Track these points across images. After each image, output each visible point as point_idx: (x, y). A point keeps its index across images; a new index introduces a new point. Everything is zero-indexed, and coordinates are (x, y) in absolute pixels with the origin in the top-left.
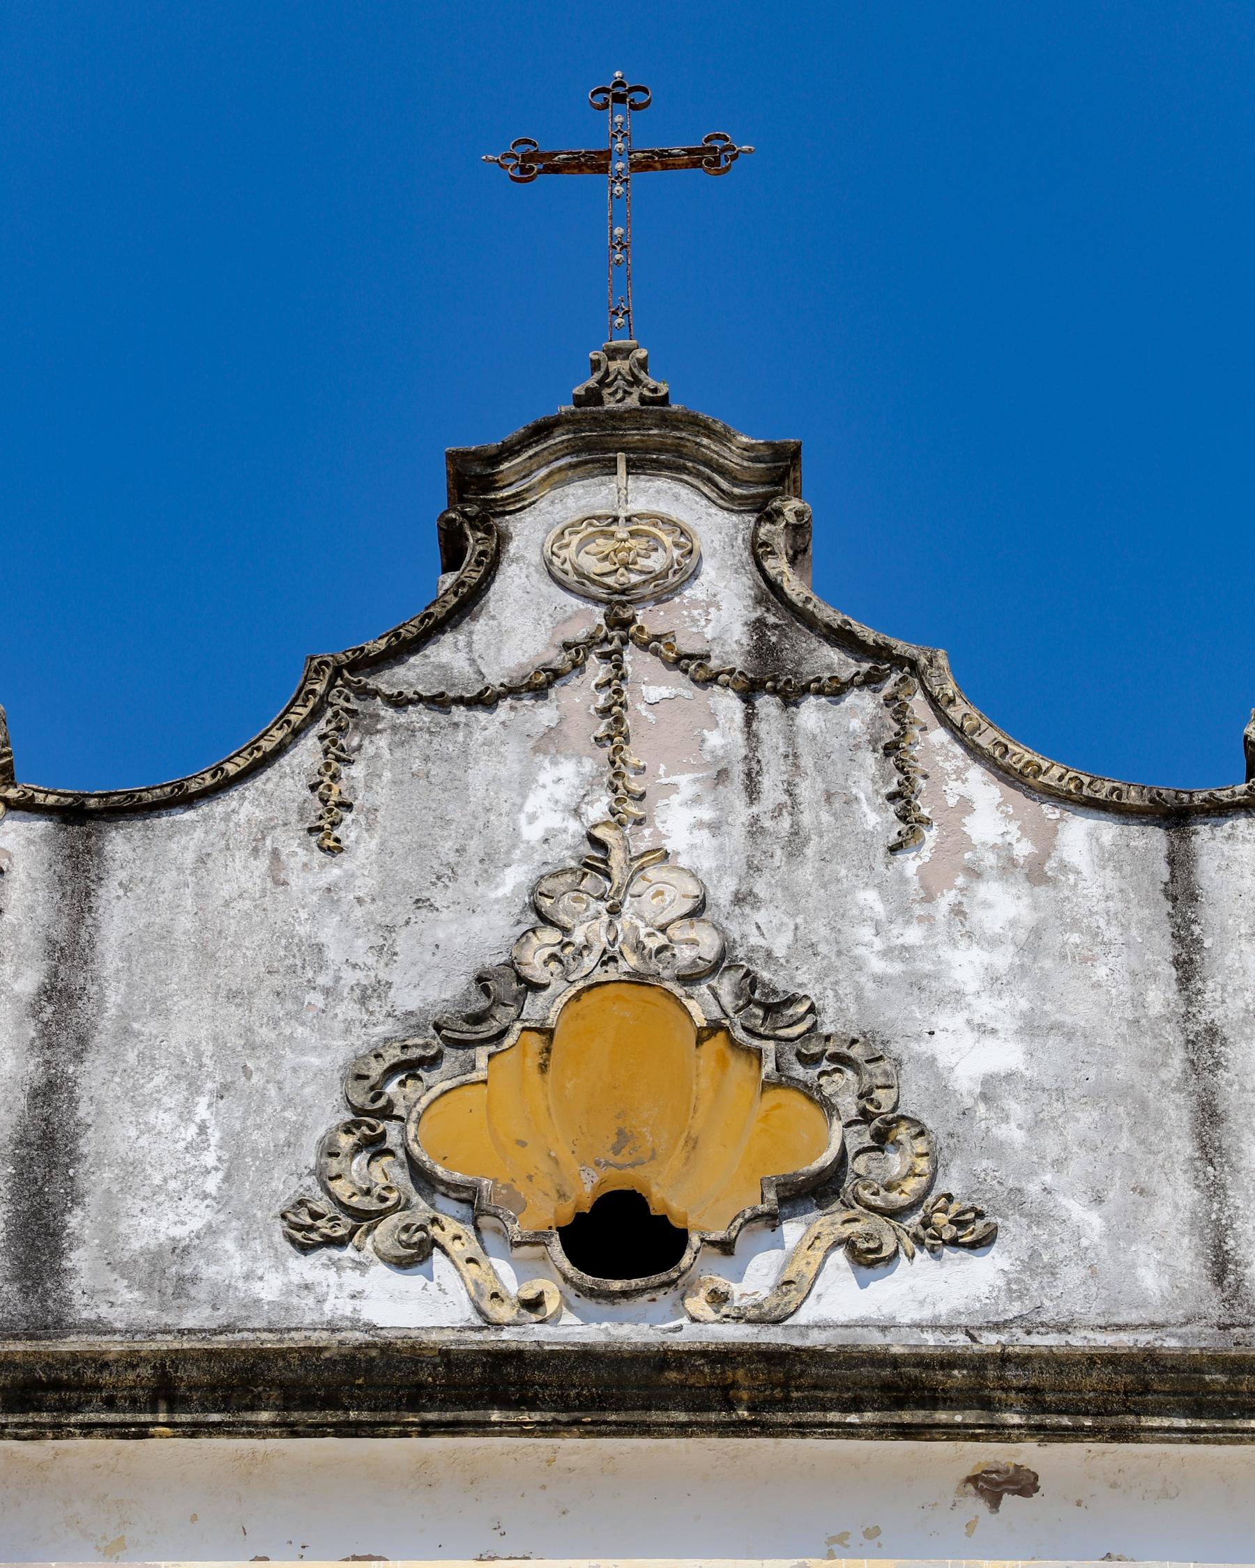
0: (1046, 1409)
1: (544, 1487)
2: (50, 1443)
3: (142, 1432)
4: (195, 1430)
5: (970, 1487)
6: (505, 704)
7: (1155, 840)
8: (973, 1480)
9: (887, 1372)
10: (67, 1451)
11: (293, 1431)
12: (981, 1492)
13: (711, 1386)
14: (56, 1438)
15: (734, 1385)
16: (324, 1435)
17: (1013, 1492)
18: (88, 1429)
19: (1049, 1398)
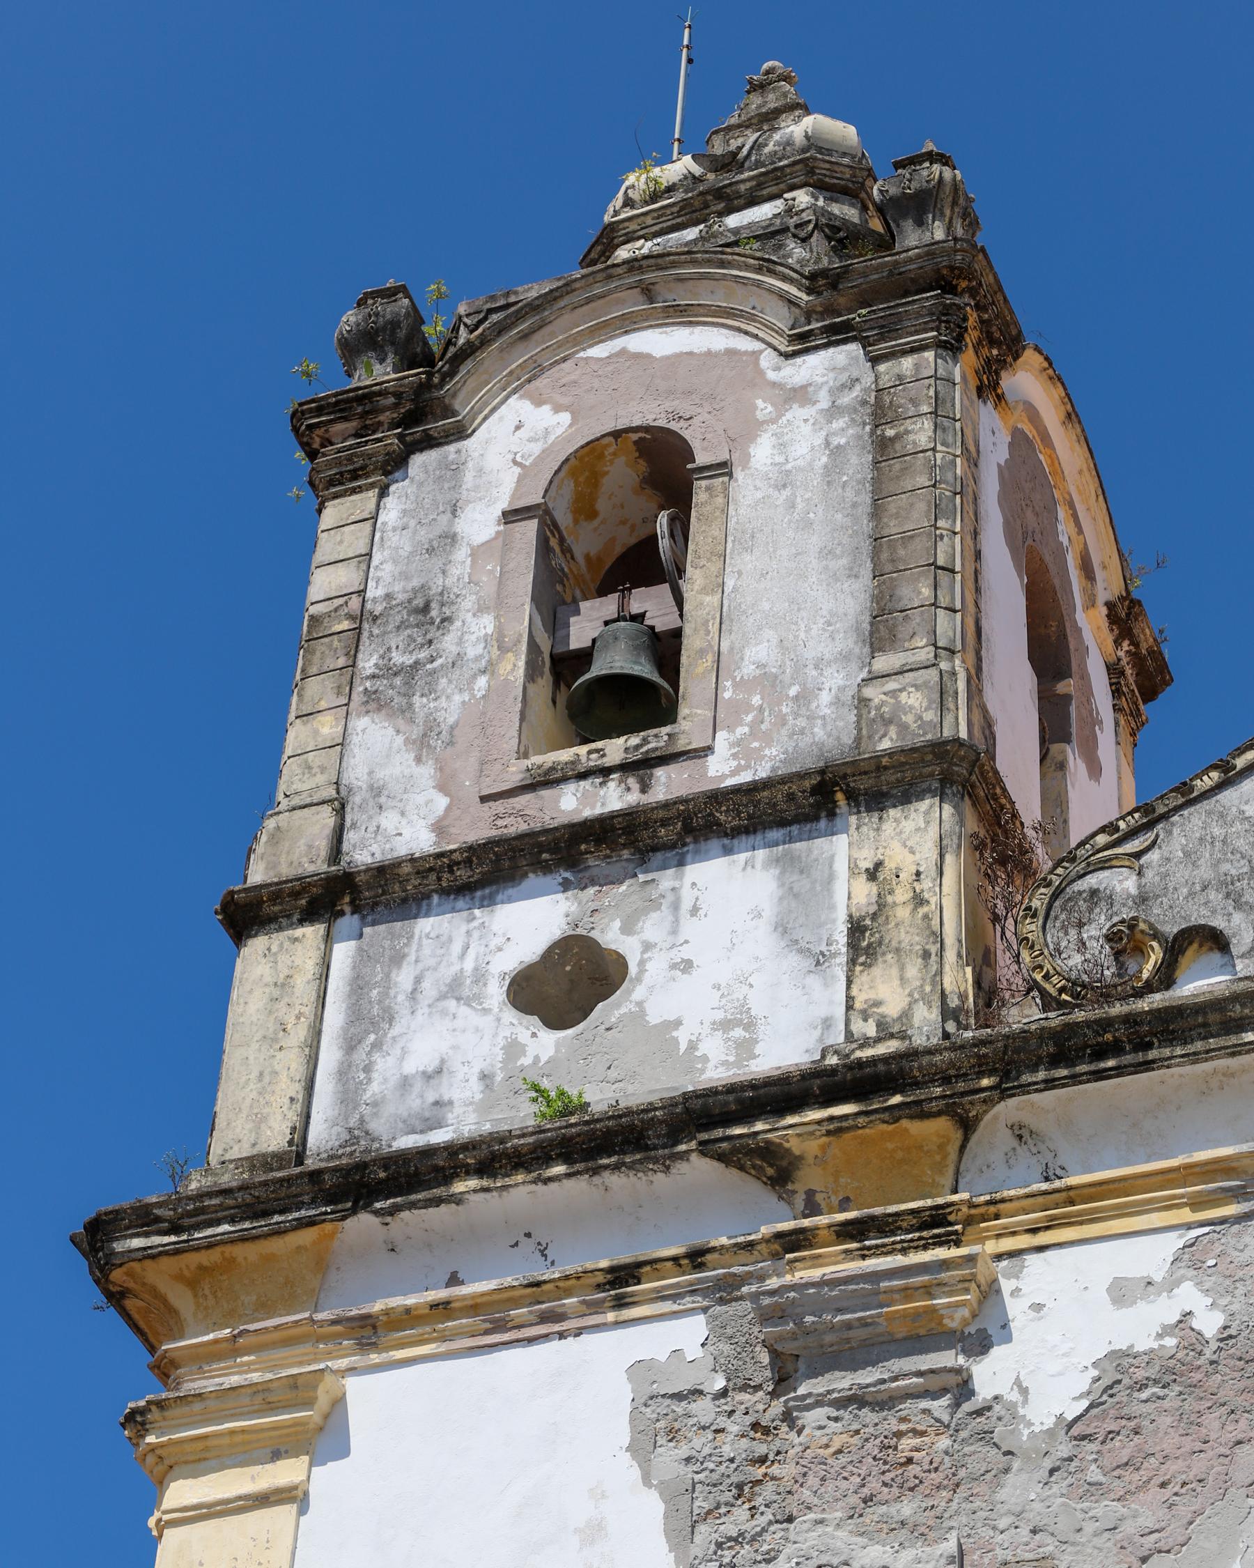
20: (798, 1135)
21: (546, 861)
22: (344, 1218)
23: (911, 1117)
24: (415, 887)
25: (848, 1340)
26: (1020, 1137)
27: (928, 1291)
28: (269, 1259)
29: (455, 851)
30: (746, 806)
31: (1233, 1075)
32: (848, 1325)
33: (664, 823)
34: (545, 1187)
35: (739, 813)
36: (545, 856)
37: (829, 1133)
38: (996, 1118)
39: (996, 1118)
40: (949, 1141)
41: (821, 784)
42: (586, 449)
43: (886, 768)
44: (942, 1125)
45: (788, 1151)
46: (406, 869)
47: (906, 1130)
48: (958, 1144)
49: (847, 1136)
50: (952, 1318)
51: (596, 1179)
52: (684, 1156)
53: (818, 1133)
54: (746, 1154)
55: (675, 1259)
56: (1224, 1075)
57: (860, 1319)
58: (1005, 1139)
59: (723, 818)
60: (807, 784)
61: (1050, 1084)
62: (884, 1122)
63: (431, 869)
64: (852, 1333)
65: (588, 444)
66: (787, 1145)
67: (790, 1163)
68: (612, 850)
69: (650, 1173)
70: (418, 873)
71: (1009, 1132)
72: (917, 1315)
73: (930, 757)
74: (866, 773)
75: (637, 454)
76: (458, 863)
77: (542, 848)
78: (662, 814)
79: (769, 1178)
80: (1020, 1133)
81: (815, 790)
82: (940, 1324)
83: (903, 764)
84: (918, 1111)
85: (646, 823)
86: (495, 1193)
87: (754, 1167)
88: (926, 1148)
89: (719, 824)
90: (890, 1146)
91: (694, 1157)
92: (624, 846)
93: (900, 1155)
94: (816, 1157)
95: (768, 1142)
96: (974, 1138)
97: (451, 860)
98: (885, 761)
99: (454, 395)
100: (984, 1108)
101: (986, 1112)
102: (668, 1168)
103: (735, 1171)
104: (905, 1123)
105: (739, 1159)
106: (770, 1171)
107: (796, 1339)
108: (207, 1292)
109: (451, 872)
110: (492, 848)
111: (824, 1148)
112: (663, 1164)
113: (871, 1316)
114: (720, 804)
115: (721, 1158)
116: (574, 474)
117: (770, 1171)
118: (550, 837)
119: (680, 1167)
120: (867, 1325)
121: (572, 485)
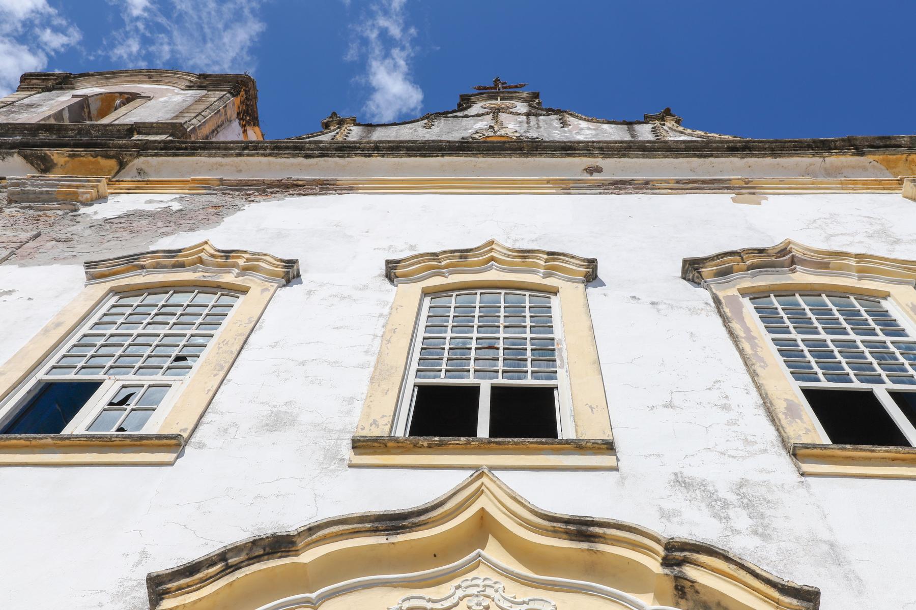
0: (604, 151)
1: (473, 171)
2: (347, 159)
3: (370, 156)
4: (383, 156)
5: (585, 171)
6: (470, 118)
7: (625, 127)
8: (585, 169)
9: (563, 144)
10: (351, 163)
11: (410, 156)
12: (588, 172)
13: (517, 148)
14: (348, 157)
15: (523, 147)
16: (416, 156)
17: (596, 172)
18: (356, 154)
19: (605, 149)
20: (58, 153)
23: (102, 156)
25: (39, 198)
26: (140, 173)
27: (77, 187)
30: (102, 130)
31: (222, 166)
32: (41, 193)
33: (72, 130)
36: (26, 132)
37: (70, 156)
38: (134, 165)
39: (134, 165)
40: (113, 169)
42: (109, 94)
43: (154, 127)
44: (113, 163)
45: (52, 160)
47: (99, 163)
48: (116, 171)
49: (77, 159)
50: (82, 197)
53: (65, 154)
54: (35, 158)
56: (219, 165)
57: (47, 191)
58: (135, 172)
60: (126, 128)
61: (156, 155)
62: (92, 156)
64: (41, 196)
65: (110, 93)
66: (52, 157)
67: (51, 166)
68: (50, 135)
71: (136, 171)
72: (69, 193)
73: (170, 127)
74: (146, 128)
77: (26, 129)
79: (41, 169)
80: (140, 172)
81: (128, 130)
82: (77, 198)
83: (160, 127)
84: (107, 157)
85: (66, 129)
87: (37, 164)
88: (104, 170)
89: (90, 134)
90: (91, 167)
91: (16, 155)
92: (55, 134)
93: (94, 170)
94: (62, 165)
95: (45, 154)
96: (123, 171)
98: (154, 125)
99: (76, 82)
100: (130, 158)
101: (130, 161)
102: (4, 158)
103: (29, 165)
104: (99, 158)
105: (32, 159)
106: (43, 167)
107: (19, 195)
111: (66, 162)
112: (3, 156)
113: (52, 191)
114: (94, 128)
115: (25, 157)
116: (103, 100)
117: (43, 167)
118: (30, 126)
120: (49, 194)
121: (101, 104)
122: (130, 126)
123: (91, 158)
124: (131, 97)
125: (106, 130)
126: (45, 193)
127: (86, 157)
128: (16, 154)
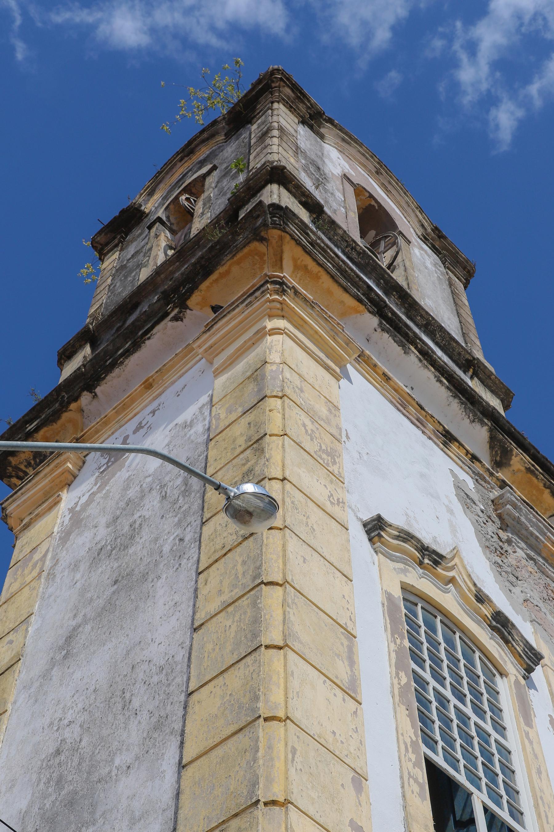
21: (381, 283)
22: (370, 312)
24: (337, 239)
28: (329, 292)
29: (359, 246)
33: (421, 316)
34: (435, 381)
35: (443, 340)
36: (382, 281)
41: (470, 361)
43: (490, 379)
45: (511, 459)
46: (340, 232)
47: (543, 493)
49: (529, 475)
51: (451, 399)
52: (483, 424)
54: (500, 446)
55: (467, 452)
59: (438, 336)
60: (467, 356)
63: (347, 241)
64: (531, 538)
67: (505, 463)
69: (467, 416)
70: (342, 237)
73: (504, 390)
75: (364, 207)
76: (356, 250)
77: (383, 278)
78: (423, 313)
79: (495, 460)
83: (496, 384)
85: (416, 309)
86: (420, 365)
90: (534, 492)
93: (534, 498)
94: (514, 471)
97: (355, 247)
102: (474, 421)
106: (498, 458)
108: (299, 275)
109: (352, 249)
110: (370, 260)
111: (519, 470)
112: (475, 419)
113: (541, 540)
114: (441, 331)
118: (389, 278)
119: (477, 426)
122: (472, 359)
123: (541, 485)
124: (377, 208)
125: (449, 344)
126: (534, 537)
127: (538, 481)
128: (487, 427)
